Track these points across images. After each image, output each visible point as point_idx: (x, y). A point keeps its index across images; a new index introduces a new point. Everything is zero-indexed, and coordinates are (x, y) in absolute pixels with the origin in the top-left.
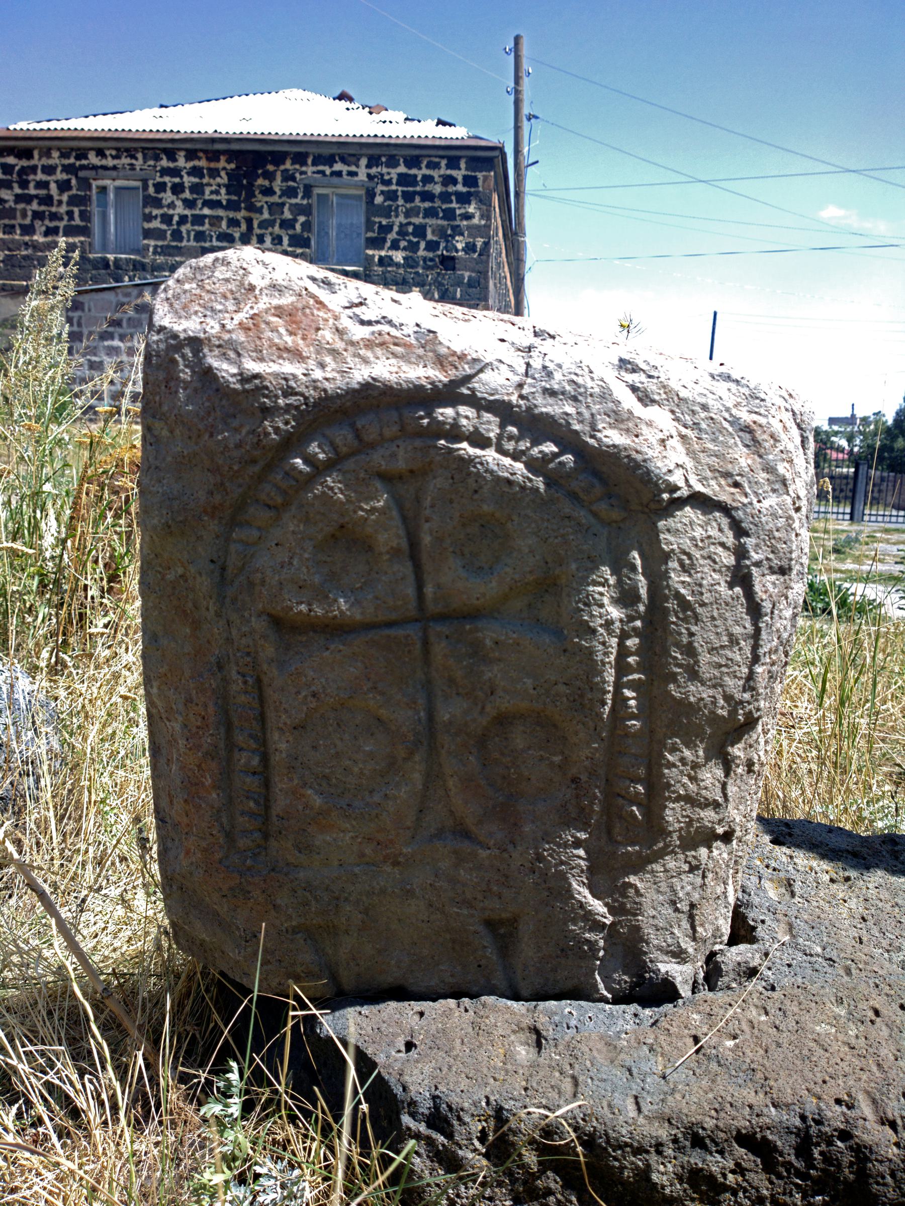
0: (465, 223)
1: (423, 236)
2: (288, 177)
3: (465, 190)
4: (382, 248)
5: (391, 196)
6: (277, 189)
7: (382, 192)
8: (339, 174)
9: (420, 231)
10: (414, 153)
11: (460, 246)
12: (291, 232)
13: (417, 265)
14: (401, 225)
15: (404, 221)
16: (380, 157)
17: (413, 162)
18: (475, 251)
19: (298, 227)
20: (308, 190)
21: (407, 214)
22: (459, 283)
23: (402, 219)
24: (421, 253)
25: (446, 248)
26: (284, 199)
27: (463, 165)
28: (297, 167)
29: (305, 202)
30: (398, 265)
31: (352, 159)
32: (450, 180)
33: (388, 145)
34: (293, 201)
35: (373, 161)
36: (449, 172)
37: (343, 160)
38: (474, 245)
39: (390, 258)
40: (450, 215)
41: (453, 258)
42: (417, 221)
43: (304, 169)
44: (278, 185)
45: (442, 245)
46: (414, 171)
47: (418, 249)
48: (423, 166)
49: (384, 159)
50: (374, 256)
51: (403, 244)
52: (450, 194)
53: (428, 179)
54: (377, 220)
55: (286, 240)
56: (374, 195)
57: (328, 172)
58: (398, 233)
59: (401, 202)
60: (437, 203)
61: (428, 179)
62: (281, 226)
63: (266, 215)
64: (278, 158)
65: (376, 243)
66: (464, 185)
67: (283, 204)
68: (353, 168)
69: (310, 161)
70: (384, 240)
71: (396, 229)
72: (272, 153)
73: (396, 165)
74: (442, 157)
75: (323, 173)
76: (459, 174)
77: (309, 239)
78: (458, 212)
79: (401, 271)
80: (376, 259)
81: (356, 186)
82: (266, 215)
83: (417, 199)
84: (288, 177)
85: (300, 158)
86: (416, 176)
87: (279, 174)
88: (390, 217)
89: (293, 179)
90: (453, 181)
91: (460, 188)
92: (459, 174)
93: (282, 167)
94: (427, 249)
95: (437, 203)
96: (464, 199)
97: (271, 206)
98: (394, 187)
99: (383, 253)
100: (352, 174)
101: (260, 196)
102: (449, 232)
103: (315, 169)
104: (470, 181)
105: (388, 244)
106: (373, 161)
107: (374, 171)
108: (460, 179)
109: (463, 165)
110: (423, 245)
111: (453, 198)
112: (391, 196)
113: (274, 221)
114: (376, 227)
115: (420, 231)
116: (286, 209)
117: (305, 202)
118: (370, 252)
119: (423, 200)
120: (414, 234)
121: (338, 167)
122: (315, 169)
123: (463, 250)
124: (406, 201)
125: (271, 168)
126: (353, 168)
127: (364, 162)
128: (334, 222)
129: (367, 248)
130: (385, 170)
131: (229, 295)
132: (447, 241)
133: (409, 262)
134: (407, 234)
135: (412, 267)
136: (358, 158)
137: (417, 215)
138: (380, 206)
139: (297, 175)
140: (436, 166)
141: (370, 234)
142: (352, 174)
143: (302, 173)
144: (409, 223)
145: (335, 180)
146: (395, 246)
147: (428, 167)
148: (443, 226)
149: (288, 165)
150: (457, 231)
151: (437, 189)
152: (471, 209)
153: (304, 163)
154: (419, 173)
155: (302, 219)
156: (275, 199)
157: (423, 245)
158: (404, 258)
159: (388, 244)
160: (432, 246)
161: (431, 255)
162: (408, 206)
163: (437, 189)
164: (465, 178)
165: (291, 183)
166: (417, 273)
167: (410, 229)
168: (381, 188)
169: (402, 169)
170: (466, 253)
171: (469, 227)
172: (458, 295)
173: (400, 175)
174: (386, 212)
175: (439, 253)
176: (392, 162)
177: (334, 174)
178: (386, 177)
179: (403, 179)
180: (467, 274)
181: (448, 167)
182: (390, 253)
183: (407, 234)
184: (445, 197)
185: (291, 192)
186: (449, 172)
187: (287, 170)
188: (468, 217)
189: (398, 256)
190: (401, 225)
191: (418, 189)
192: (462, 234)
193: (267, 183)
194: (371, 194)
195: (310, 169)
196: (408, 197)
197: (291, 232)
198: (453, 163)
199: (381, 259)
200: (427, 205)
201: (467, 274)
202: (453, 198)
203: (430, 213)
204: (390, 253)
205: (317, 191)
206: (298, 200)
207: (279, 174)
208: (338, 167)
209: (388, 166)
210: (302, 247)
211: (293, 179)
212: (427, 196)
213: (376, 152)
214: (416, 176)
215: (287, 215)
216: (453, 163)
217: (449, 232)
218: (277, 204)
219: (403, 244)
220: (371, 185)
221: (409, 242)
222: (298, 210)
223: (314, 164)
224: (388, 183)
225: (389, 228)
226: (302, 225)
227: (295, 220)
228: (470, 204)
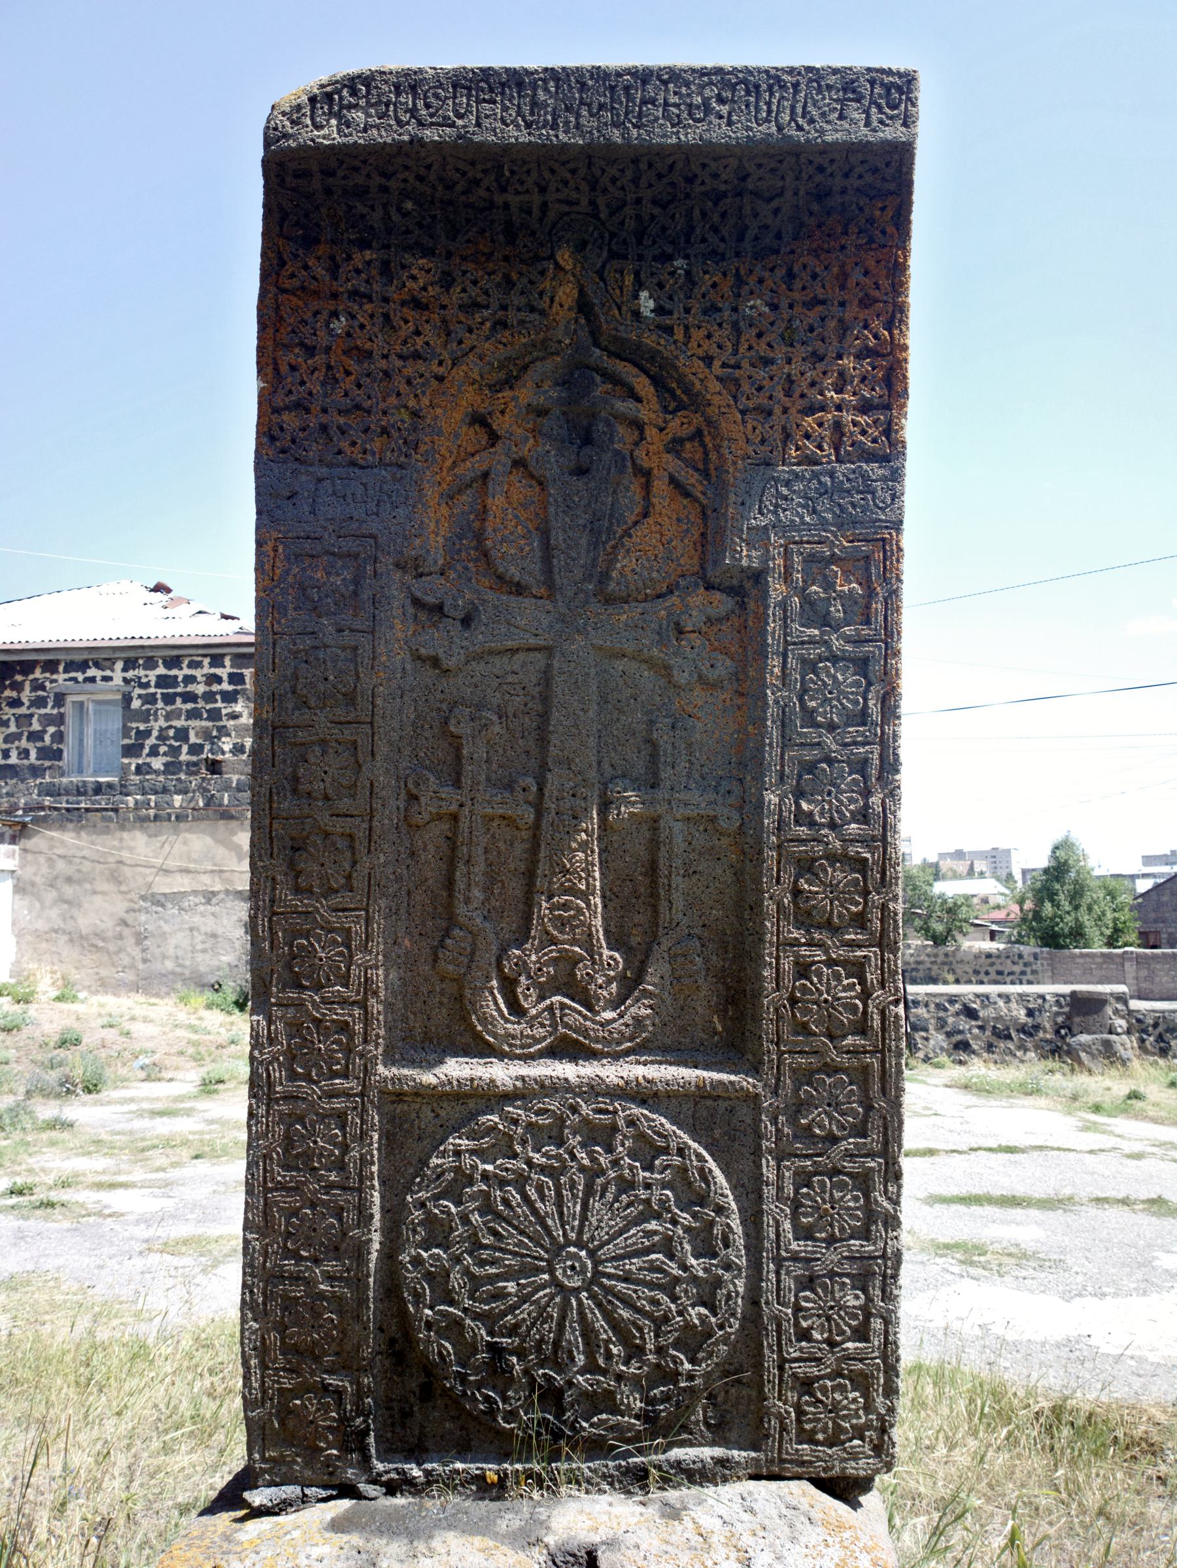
0: (232, 722)
1: (186, 739)
2: (38, 686)
3: (231, 688)
4: (139, 756)
5: (150, 699)
6: (25, 700)
7: (140, 696)
8: (92, 680)
9: (182, 734)
10: (174, 655)
11: (226, 748)
12: (39, 744)
13: (180, 770)
14: (161, 730)
15: (165, 725)
16: (137, 659)
17: (173, 662)
19: (47, 738)
20: (60, 699)
21: (168, 717)
22: (227, 787)
23: (161, 723)
24: (184, 757)
25: (211, 751)
26: (33, 710)
27: (227, 662)
28: (47, 675)
29: (55, 711)
30: (157, 772)
31: (108, 663)
32: (215, 679)
33: (143, 647)
34: (43, 711)
35: (130, 664)
36: (213, 671)
37: (97, 665)
38: (243, 746)
39: (149, 765)
40: (215, 715)
41: (220, 762)
42: (178, 723)
43: (55, 677)
44: (26, 695)
45: (207, 747)
46: (174, 672)
48: (184, 665)
49: (141, 662)
51: (163, 749)
52: (215, 693)
53: (190, 679)
54: (134, 725)
55: (33, 754)
56: (131, 699)
57: (80, 679)
58: (157, 738)
59: (160, 704)
60: (201, 704)
61: (190, 679)
62: (28, 739)
63: (13, 728)
64: (27, 667)
65: (130, 751)
66: (230, 683)
67: (32, 715)
68: (108, 673)
69: (61, 668)
70: (142, 746)
71: (155, 733)
72: (20, 663)
73: (155, 667)
74: (205, 656)
75: (75, 679)
76: (223, 673)
77: (60, 751)
78: (224, 712)
79: (161, 778)
80: (133, 768)
81: (111, 691)
82: (13, 728)
83: (179, 700)
84: (38, 686)
85: (51, 666)
86: (176, 677)
87: (27, 684)
88: (148, 721)
89: (43, 688)
90: (218, 679)
91: (226, 686)
92: (223, 673)
93: (31, 677)
94: (189, 753)
95: (201, 704)
96: (230, 698)
97: (19, 719)
98: (152, 690)
99: (140, 761)
100: (106, 679)
101: (7, 709)
102: (215, 733)
103: (67, 676)
104: (236, 679)
105: (146, 750)
106: (130, 664)
107: (130, 674)
108: (225, 677)
109: (227, 662)
110: (185, 749)
111: (218, 697)
112: (150, 699)
113: (21, 734)
114: (133, 733)
115: (182, 734)
116: (35, 720)
117: (55, 711)
118: (126, 761)
119: (185, 702)
120: (175, 738)
121: (91, 672)
122: (67, 676)
124: (166, 704)
125: (19, 678)
126: (108, 673)
127: (119, 665)
128: (90, 730)
129: (124, 756)
130: (142, 673)
132: (213, 743)
133: (171, 768)
134: (167, 738)
136: (113, 661)
137: (179, 718)
138: (137, 712)
139: (47, 684)
140: (198, 665)
141: (127, 741)
142: (106, 679)
143: (53, 681)
144: (170, 727)
145: (89, 686)
146: (154, 752)
147: (189, 666)
149: (38, 674)
150: (223, 731)
151: (200, 689)
152: (238, 707)
153: (54, 671)
154: (180, 674)
155: (52, 729)
156: (23, 710)
157: (185, 749)
158: (165, 765)
159: (146, 750)
160: (195, 749)
161: (194, 758)
162: (169, 708)
163: (200, 689)
164: (230, 675)
165: (40, 693)
166: (179, 780)
167: (171, 733)
168: (138, 691)
169: (161, 670)
171: (236, 728)
172: (226, 801)
173: (159, 677)
174: (145, 717)
176: (150, 663)
177: (86, 680)
178: (144, 680)
179: (162, 681)
180: (235, 778)
181: (211, 665)
182: (148, 760)
183: (167, 738)
184: (209, 697)
185: (40, 702)
186: (213, 671)
187: (36, 680)
188: (234, 716)
190: (161, 730)
191: (179, 690)
192: (229, 735)
193: (14, 694)
194: (127, 699)
195: (61, 677)
196: (169, 699)
197: (39, 744)
198: (217, 661)
199: (138, 767)
200: (190, 706)
201: (235, 778)
202: (218, 697)
203: (193, 714)
204: (148, 760)
205: (70, 699)
206: (48, 710)
207: (27, 684)
208: (91, 672)
209: (145, 669)
211: (43, 688)
212: (189, 697)
213: (132, 654)
214: (176, 677)
215: (36, 726)
216: (217, 661)
217: (215, 733)
218: (26, 716)
219: (163, 749)
220: (128, 689)
221: (170, 746)
222: (47, 720)
223: (66, 671)
224: (147, 685)
225: (148, 733)
226: (52, 736)
227: (44, 732)
228: (236, 701)
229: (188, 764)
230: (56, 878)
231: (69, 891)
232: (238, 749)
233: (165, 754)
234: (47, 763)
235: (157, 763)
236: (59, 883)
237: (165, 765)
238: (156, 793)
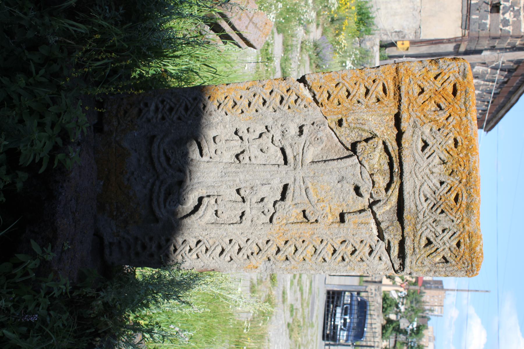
11: (507, 16)
18: (503, 26)
38: (507, 25)
41: (498, 11)
102: (516, 8)
123: (504, 18)
148: (519, 3)
170: (502, 20)
175: (502, 3)
201: (488, 22)
217: (516, 8)
232: (506, 23)
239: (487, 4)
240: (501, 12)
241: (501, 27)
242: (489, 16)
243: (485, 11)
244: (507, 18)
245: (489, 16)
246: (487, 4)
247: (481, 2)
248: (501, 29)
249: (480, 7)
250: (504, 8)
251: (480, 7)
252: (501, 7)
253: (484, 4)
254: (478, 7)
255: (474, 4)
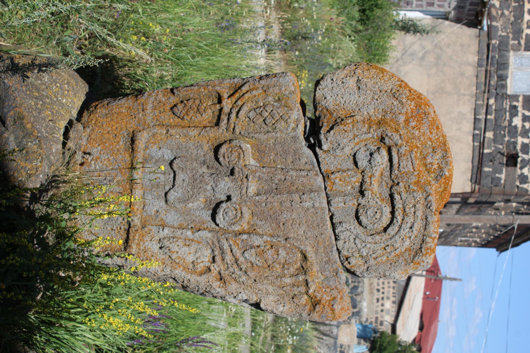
4: (524, 108)
13: (511, 137)
18: (521, 183)
30: (510, 121)
38: (525, 183)
39: (516, 115)
41: (515, 165)
47: (523, 137)
50: (518, 101)
80: (515, 103)
99: (520, 109)
118: (521, 99)
123: (522, 174)
131: (274, 126)
135: (509, 132)
166: (505, 136)
170: (519, 176)
175: (520, 154)
182: (520, 114)
189: (517, 121)
199: (515, 107)
201: (503, 176)
210: (525, 44)
229: (515, 143)
230: (441, 48)
231: (431, 58)
233: (523, 126)
234: (523, 42)
235: (517, 121)
236: (438, 51)
237: (516, 127)
238: (496, 119)
239: (503, 154)
240: (519, 166)
241: (518, 183)
242: (504, 170)
243: (500, 163)
244: (526, 174)
245: (504, 170)
246: (503, 154)
247: (495, 153)
248: (518, 187)
249: (494, 157)
250: (522, 161)
251: (494, 157)
252: (519, 160)
253: (499, 155)
254: (491, 157)
255: (487, 153)
